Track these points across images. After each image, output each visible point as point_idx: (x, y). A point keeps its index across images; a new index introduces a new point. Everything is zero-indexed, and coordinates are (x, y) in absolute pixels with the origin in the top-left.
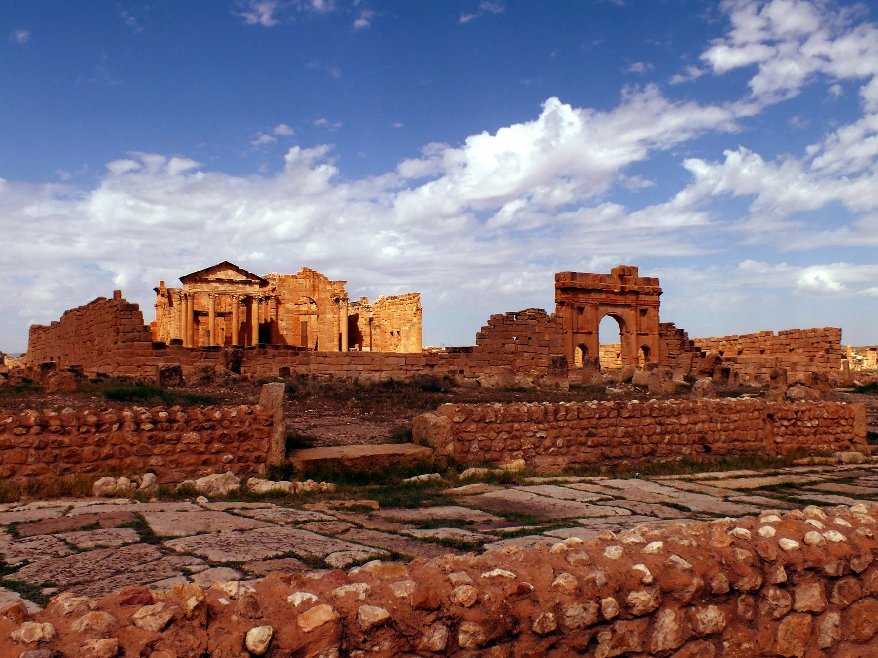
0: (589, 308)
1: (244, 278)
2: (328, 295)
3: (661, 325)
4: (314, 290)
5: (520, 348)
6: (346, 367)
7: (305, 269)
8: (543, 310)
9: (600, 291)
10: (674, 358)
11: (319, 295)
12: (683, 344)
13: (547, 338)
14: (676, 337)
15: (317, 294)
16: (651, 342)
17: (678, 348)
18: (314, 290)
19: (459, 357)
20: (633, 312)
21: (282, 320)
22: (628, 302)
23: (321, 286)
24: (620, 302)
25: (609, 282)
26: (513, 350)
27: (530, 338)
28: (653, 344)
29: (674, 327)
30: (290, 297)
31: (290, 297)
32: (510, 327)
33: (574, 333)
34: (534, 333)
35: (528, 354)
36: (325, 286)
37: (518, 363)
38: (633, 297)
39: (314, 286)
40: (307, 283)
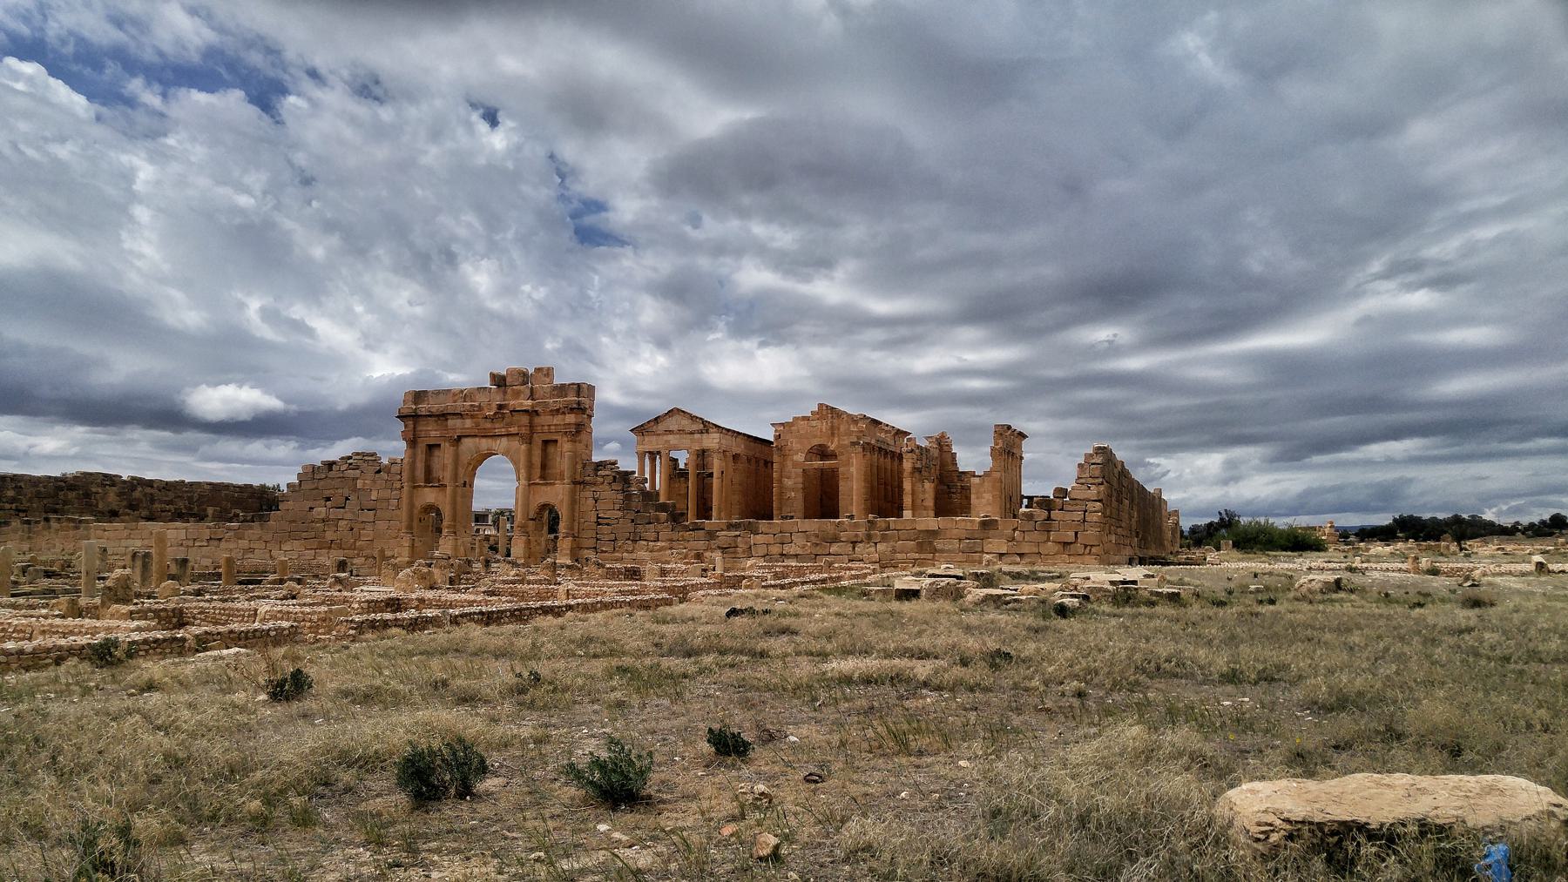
4: (833, 434)
5: (334, 514)
6: (124, 543)
7: (821, 405)
9: (460, 415)
10: (608, 524)
11: (839, 441)
12: (628, 497)
13: (373, 498)
14: (615, 486)
15: (836, 439)
17: (617, 507)
18: (833, 434)
19: (251, 528)
23: (842, 428)
25: (481, 399)
26: (323, 516)
27: (347, 499)
30: (799, 446)
31: (799, 446)
32: (322, 483)
33: (415, 487)
35: (346, 522)
36: (849, 428)
37: (329, 535)
39: (832, 428)
40: (824, 426)
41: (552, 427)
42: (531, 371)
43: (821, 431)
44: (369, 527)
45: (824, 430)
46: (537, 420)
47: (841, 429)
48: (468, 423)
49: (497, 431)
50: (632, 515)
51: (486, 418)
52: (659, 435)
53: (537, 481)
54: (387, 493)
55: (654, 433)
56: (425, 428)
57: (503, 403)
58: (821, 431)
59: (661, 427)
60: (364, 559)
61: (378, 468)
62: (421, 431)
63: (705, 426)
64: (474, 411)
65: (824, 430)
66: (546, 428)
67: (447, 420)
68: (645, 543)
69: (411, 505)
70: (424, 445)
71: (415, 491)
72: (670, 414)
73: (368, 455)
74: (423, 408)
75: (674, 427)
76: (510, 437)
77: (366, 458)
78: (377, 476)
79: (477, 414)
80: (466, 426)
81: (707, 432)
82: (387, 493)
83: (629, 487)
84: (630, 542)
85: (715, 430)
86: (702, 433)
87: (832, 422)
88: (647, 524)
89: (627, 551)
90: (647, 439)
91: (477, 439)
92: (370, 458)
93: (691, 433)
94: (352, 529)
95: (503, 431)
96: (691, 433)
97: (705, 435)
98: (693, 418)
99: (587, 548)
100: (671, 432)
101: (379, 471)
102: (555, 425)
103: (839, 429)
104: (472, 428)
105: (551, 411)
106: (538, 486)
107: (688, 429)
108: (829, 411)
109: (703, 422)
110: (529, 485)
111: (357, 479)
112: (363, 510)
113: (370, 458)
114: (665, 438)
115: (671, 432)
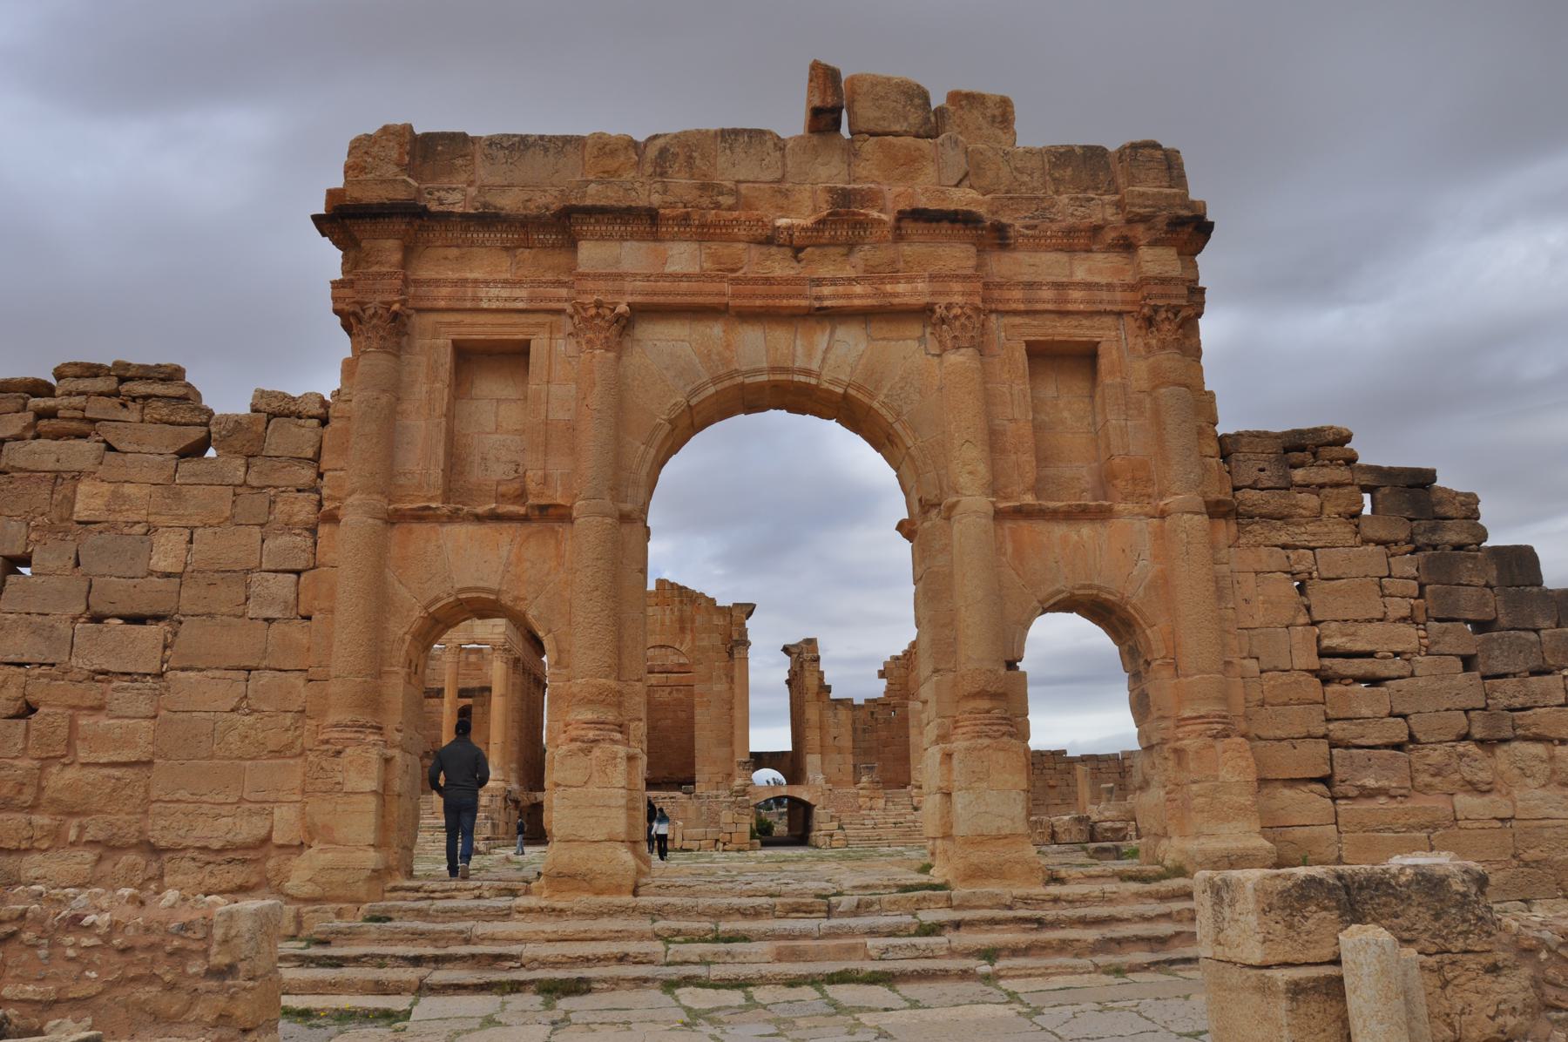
0: (563, 346)
2: (717, 639)
3: (1228, 448)
4: (682, 630)
8: (173, 374)
10: (1375, 681)
11: (693, 640)
13: (161, 562)
15: (688, 637)
16: (1146, 567)
17: (1400, 607)
18: (682, 630)
20: (960, 359)
22: (906, 292)
23: (699, 620)
24: (830, 296)
28: (1163, 584)
29: (1351, 460)
33: (394, 519)
34: (65, 525)
38: (956, 255)
39: (682, 620)
41: (1076, 294)
42: (938, 100)
43: (663, 624)
44: (131, 701)
45: (668, 622)
46: (1003, 265)
47: (697, 624)
48: (682, 257)
49: (827, 290)
50: (1462, 638)
51: (769, 241)
53: (1029, 499)
54: (237, 546)
56: (451, 275)
57: (849, 187)
58: (663, 624)
60: (89, 855)
61: (196, 433)
62: (437, 283)
64: (718, 206)
65: (668, 622)
66: (1047, 294)
67: (572, 244)
68: (1539, 749)
69: (380, 603)
70: (444, 343)
71: (396, 533)
73: (147, 374)
74: (455, 198)
76: (880, 329)
77: (140, 388)
78: (187, 466)
79: (728, 224)
80: (669, 269)
82: (237, 546)
83: (1433, 530)
84: (1472, 748)
87: (681, 610)
88: (1533, 673)
89: (1473, 787)
91: (716, 330)
92: (159, 389)
94: (29, 710)
95: (861, 296)
99: (1292, 782)
101: (195, 451)
102: (1089, 286)
103: (693, 621)
104: (702, 277)
105: (1070, 232)
106: (1040, 526)
108: (676, 592)
110: (999, 515)
111: (77, 476)
112: (98, 619)
113: (159, 389)
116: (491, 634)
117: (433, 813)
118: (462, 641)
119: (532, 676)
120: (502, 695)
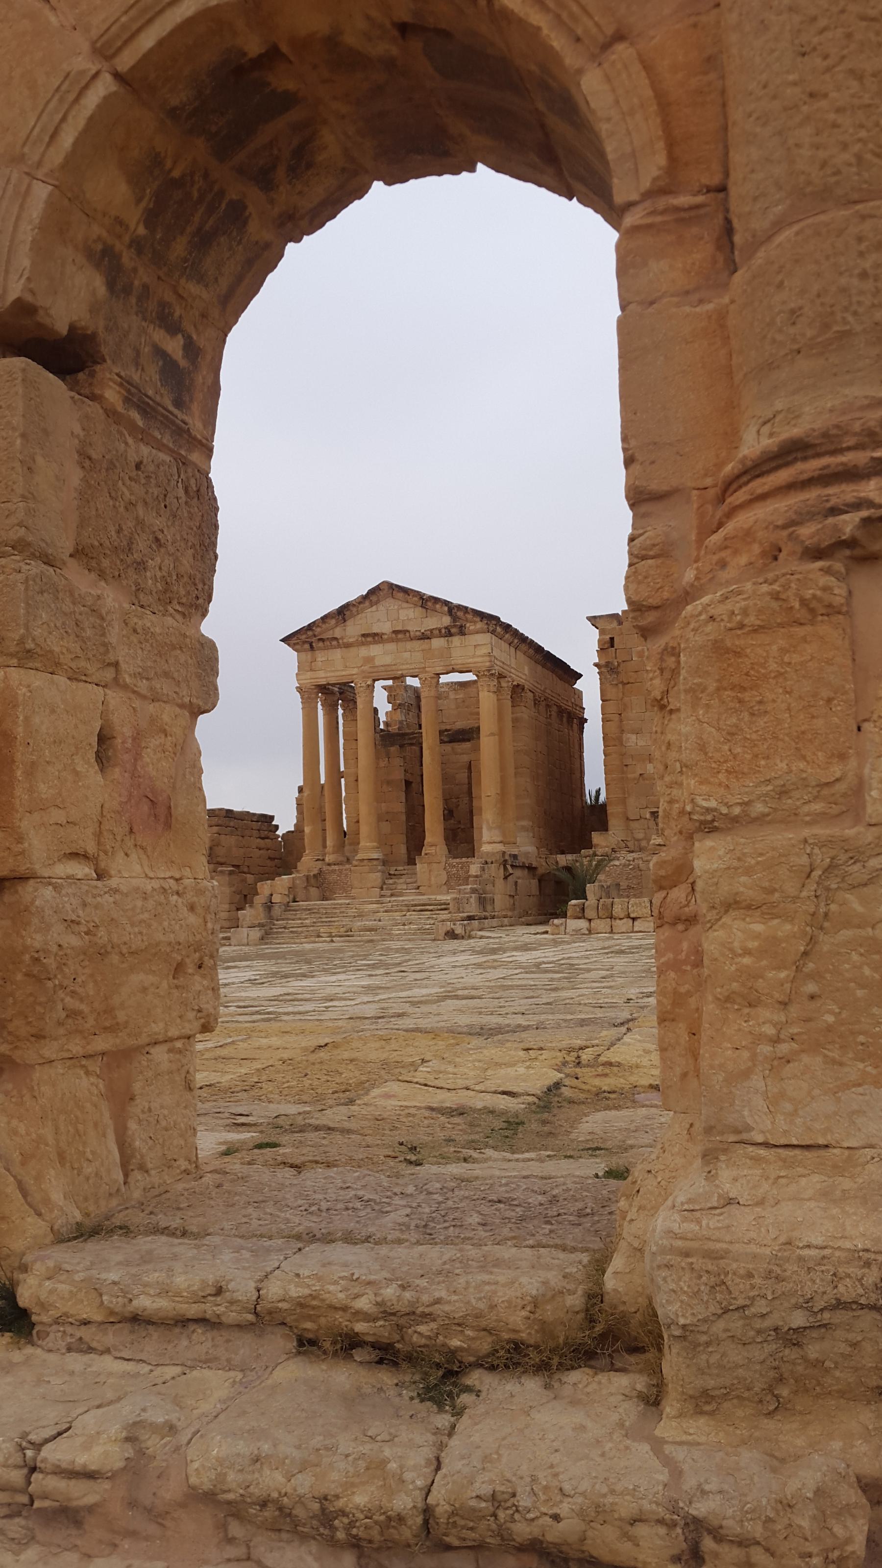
1: (447, 620)
21: (637, 732)
52: (348, 646)
55: (335, 643)
59: (352, 629)
63: (455, 618)
72: (374, 598)
75: (385, 628)
81: (462, 632)
85: (480, 625)
86: (450, 634)
90: (321, 656)
93: (425, 637)
96: (425, 637)
97: (456, 640)
98: (427, 602)
100: (375, 638)
107: (414, 628)
109: (453, 610)
114: (364, 652)
115: (375, 638)
116: (474, 656)
117: (418, 888)
118: (438, 670)
119: (555, 708)
120: (492, 734)
